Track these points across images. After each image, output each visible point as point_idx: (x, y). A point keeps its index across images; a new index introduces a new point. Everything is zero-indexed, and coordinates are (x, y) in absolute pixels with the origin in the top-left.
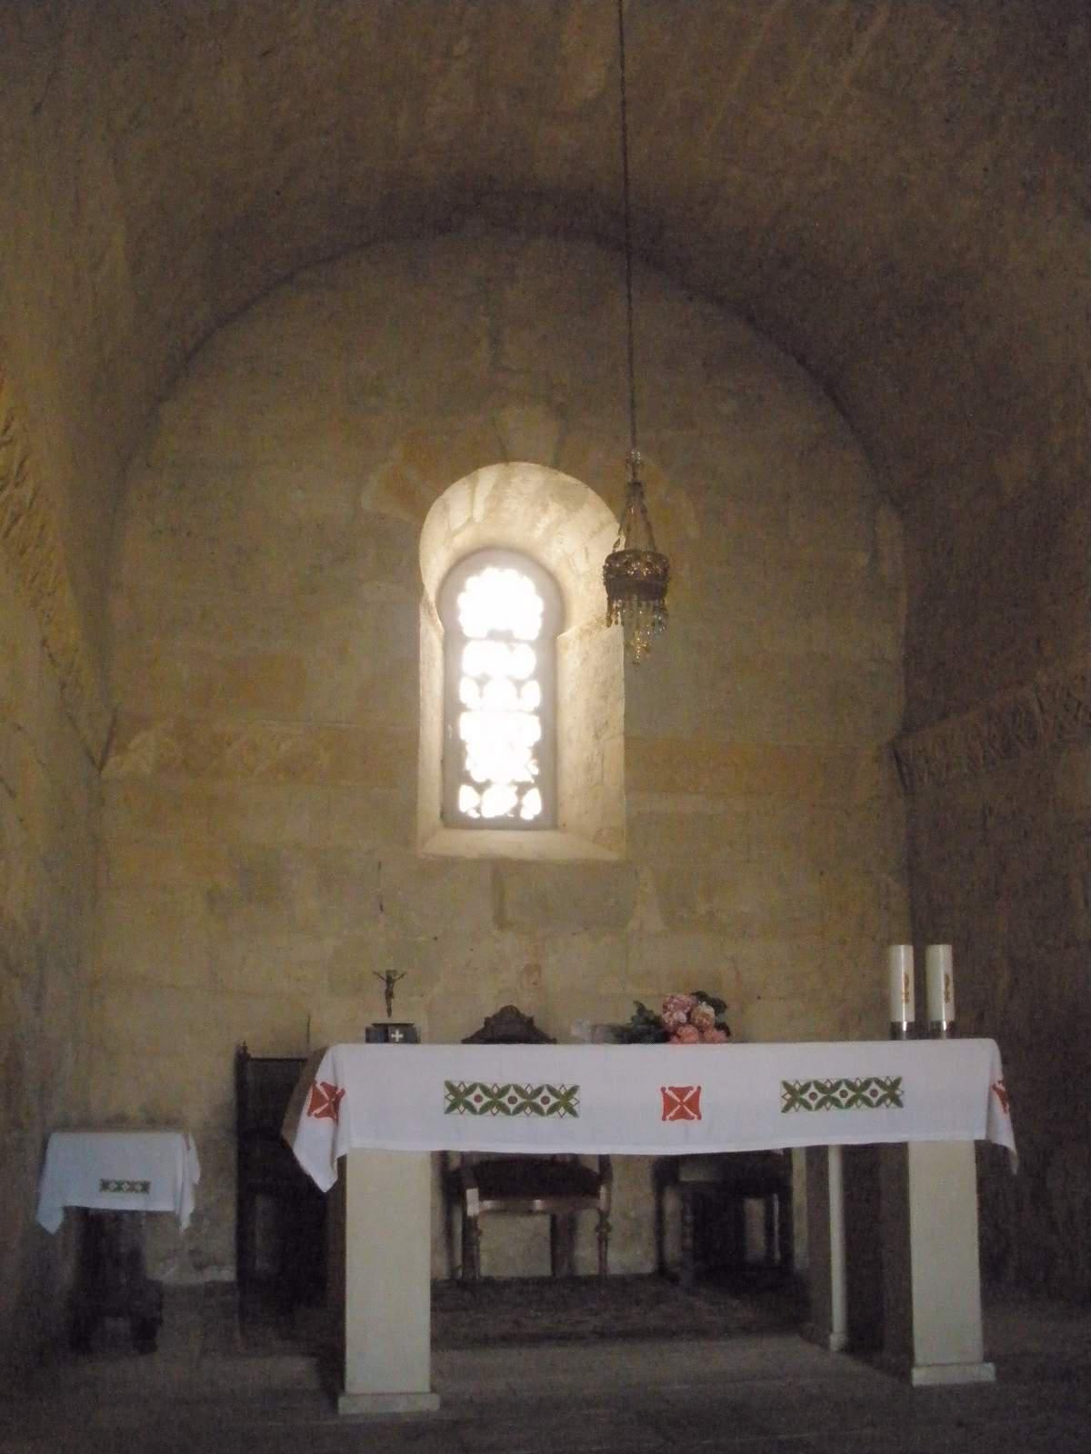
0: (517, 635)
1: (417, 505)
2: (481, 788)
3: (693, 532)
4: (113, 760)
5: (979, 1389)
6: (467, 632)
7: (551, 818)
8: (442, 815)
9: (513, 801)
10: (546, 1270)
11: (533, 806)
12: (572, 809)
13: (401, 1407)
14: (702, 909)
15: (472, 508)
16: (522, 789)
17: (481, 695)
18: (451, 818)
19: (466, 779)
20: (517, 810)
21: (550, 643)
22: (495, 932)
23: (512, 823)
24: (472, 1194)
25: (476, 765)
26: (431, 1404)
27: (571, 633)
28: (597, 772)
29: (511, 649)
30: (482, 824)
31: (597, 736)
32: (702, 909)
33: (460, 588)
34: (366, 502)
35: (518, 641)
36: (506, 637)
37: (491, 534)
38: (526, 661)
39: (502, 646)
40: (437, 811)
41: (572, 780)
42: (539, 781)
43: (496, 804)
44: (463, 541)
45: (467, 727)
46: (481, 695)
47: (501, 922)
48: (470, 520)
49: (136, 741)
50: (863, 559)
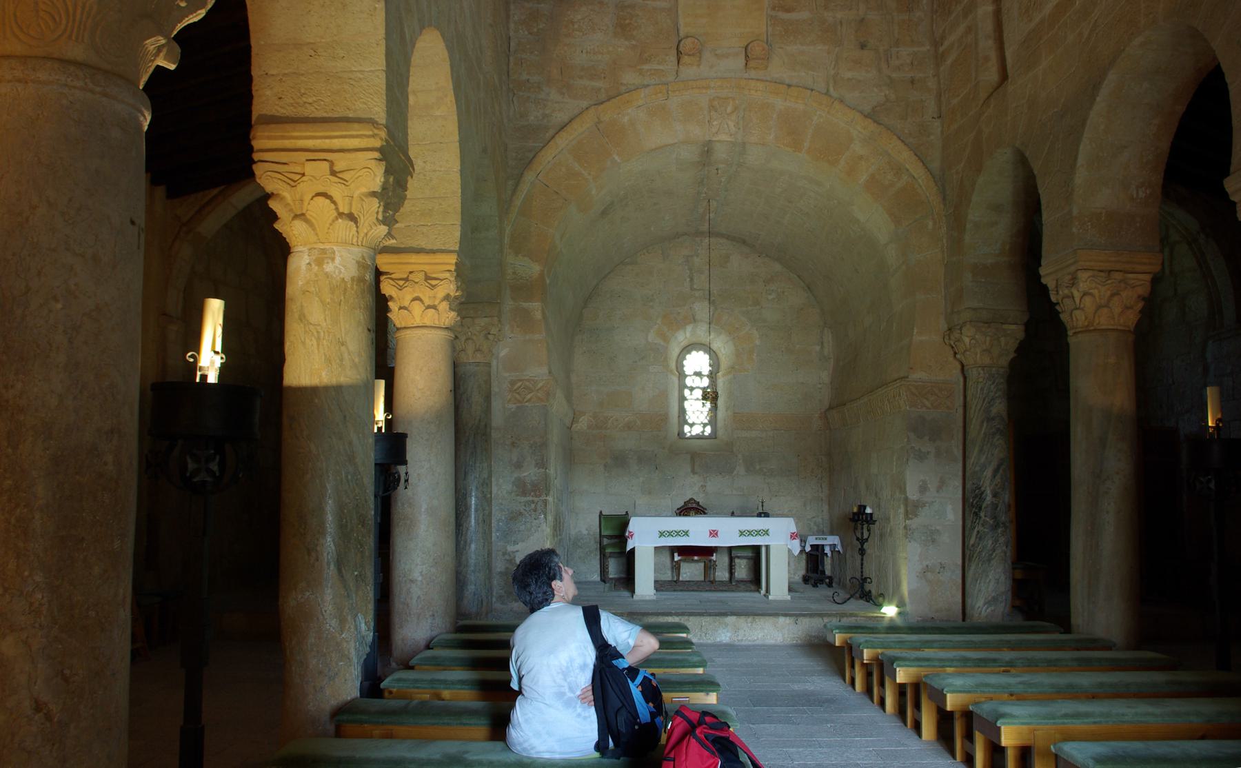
0: (703, 373)
1: (666, 340)
2: (692, 425)
3: (758, 342)
4: (574, 426)
5: (785, 602)
6: (687, 373)
7: (713, 435)
8: (678, 435)
9: (702, 429)
10: (702, 579)
11: (708, 430)
12: (720, 433)
13: (647, 598)
14: (758, 467)
15: (685, 334)
16: (705, 425)
17: (691, 394)
18: (681, 434)
19: (686, 422)
20: (703, 432)
21: (712, 376)
22: (692, 476)
23: (699, 437)
24: (676, 555)
25: (691, 417)
26: (655, 598)
27: (720, 374)
28: (726, 423)
29: (701, 379)
30: (692, 438)
31: (727, 411)
32: (758, 467)
33: (684, 358)
34: (650, 340)
35: (704, 376)
36: (698, 374)
37: (694, 340)
38: (705, 382)
39: (698, 378)
40: (677, 433)
41: (720, 424)
42: (710, 423)
43: (697, 430)
44: (684, 344)
45: (686, 404)
46: (691, 394)
47: (694, 472)
48: (686, 338)
49: (581, 420)
50: (818, 348)
